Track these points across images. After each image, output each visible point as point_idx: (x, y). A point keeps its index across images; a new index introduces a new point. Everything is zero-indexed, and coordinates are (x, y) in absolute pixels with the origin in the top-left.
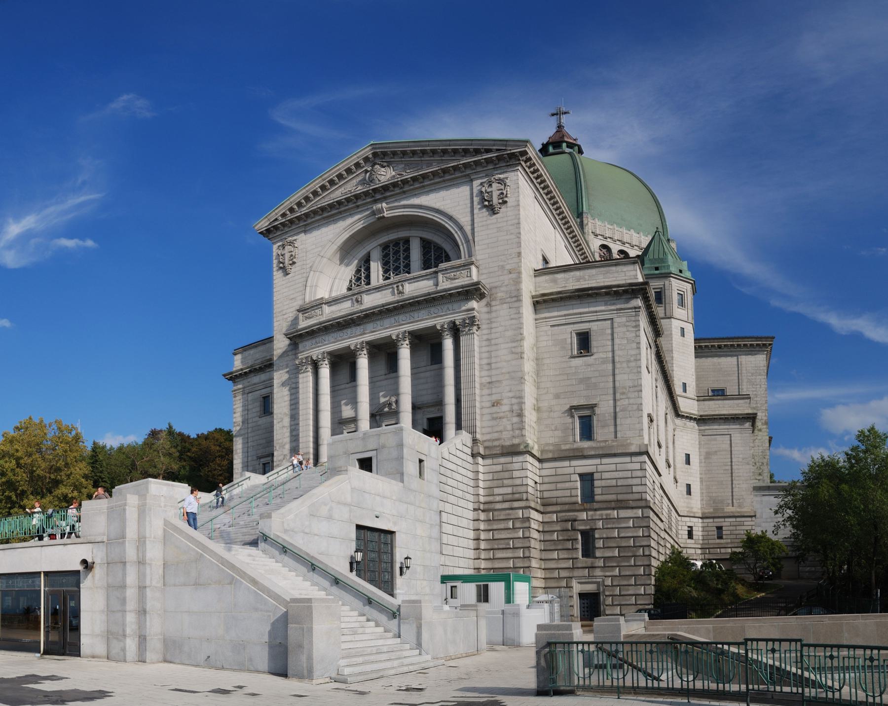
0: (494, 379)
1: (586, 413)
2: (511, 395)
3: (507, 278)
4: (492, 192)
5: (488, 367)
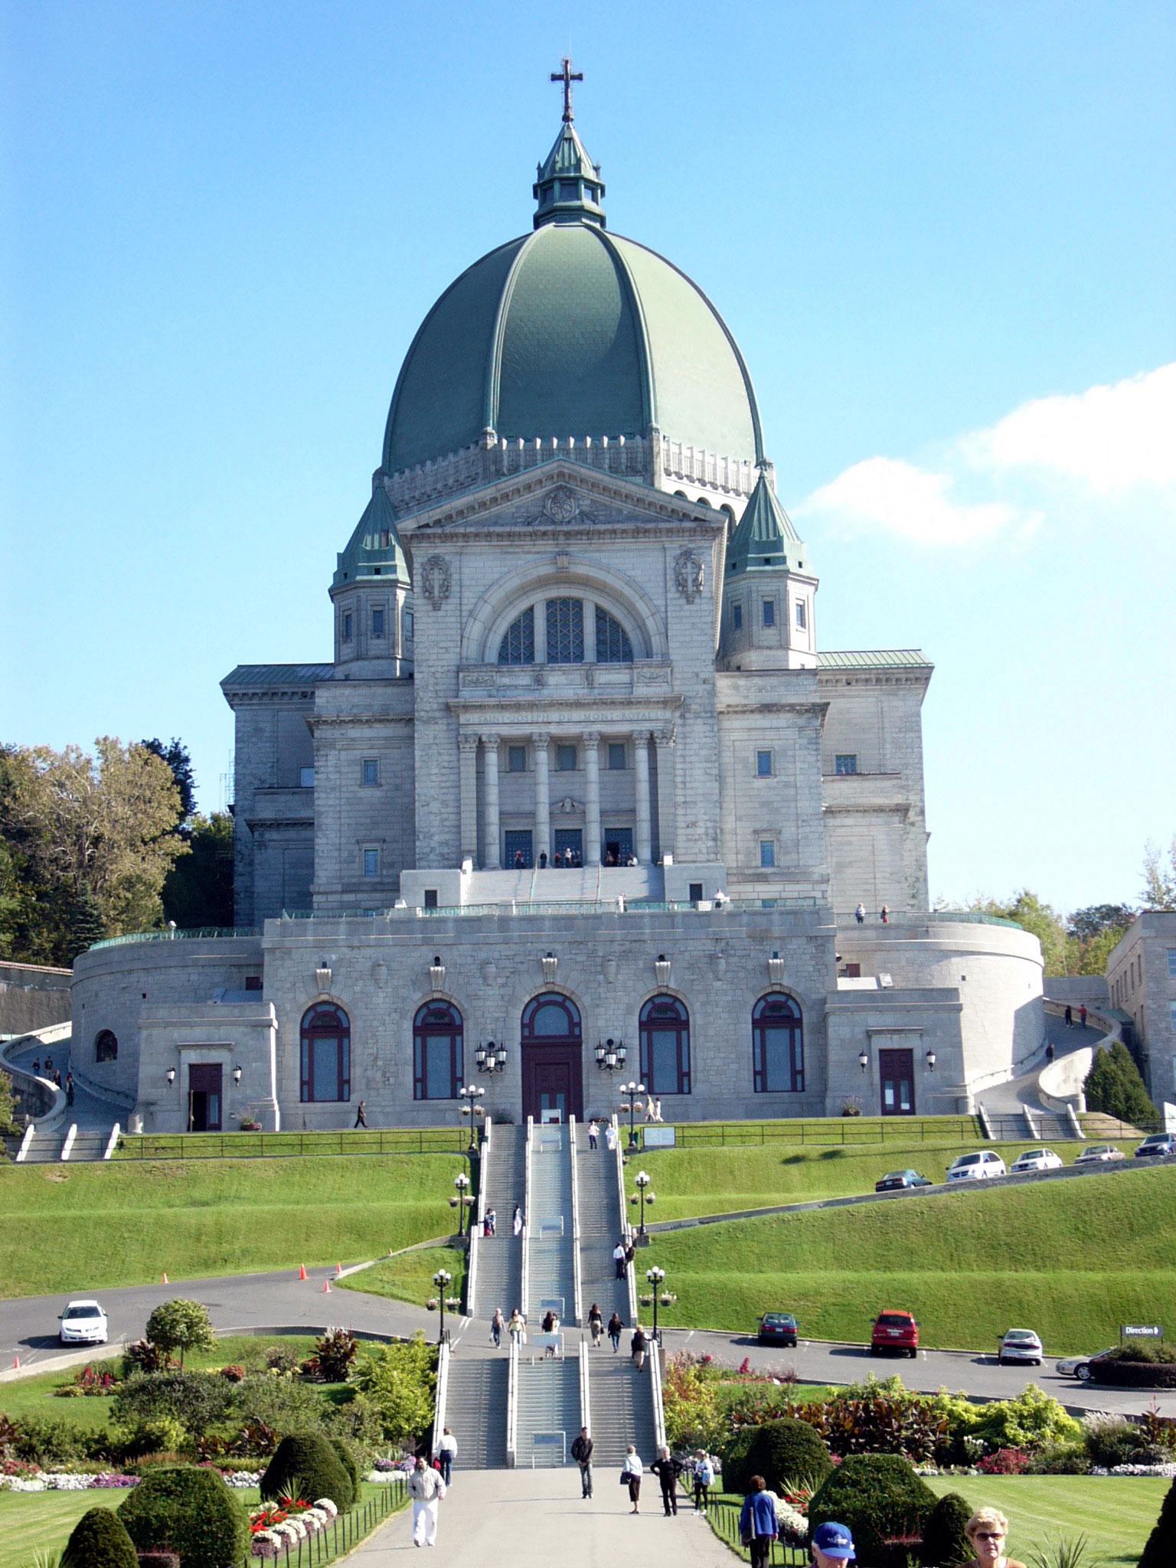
0: (689, 799)
1: (766, 837)
2: (706, 817)
3: (701, 688)
5: (680, 786)
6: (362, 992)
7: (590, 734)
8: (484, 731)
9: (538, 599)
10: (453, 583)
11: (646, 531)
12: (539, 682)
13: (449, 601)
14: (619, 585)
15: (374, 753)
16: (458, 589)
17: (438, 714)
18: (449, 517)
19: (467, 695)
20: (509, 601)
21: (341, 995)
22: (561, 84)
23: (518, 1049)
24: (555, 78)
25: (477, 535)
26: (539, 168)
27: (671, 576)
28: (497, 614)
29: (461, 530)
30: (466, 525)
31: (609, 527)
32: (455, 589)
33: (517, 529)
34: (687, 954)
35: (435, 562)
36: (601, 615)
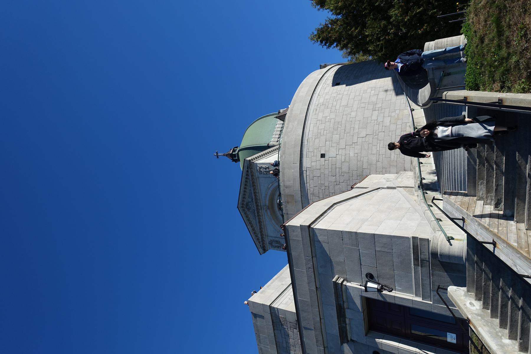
4: (264, 171)
10: (276, 239)
13: (281, 241)
16: (277, 238)
25: (261, 232)
26: (233, 161)
27: (265, 176)
31: (253, 195)
32: (277, 239)
33: (257, 221)
35: (271, 243)
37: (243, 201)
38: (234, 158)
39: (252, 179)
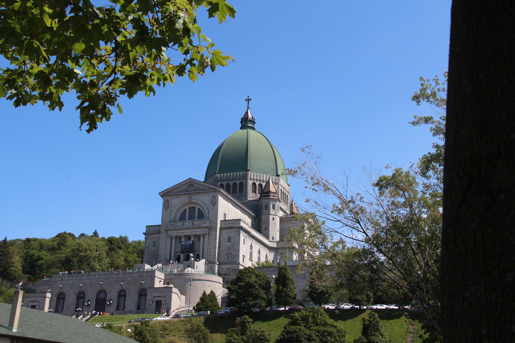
0: (211, 247)
6: (68, 290)
7: (192, 235)
8: (172, 235)
9: (187, 207)
11: (206, 192)
12: (183, 224)
14: (201, 203)
15: (156, 240)
17: (164, 232)
18: (169, 192)
19: (170, 228)
20: (181, 207)
21: (64, 290)
22: (247, 102)
23: (95, 302)
24: (246, 100)
25: (174, 195)
28: (178, 210)
29: (171, 194)
30: (172, 193)
32: (170, 206)
33: (181, 193)
34: (127, 281)
36: (199, 210)
37: (194, 183)
38: (243, 122)
39: (208, 192)
